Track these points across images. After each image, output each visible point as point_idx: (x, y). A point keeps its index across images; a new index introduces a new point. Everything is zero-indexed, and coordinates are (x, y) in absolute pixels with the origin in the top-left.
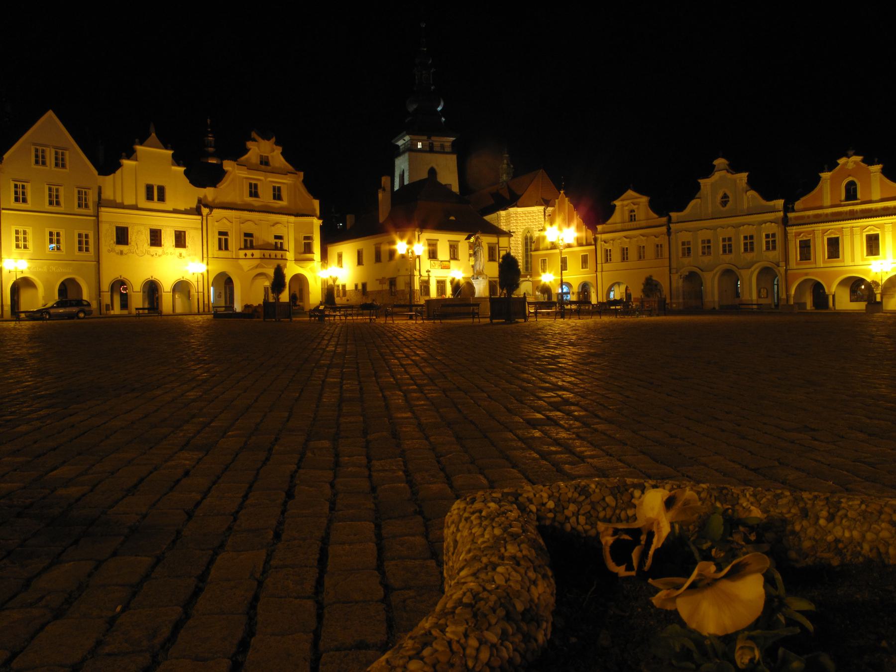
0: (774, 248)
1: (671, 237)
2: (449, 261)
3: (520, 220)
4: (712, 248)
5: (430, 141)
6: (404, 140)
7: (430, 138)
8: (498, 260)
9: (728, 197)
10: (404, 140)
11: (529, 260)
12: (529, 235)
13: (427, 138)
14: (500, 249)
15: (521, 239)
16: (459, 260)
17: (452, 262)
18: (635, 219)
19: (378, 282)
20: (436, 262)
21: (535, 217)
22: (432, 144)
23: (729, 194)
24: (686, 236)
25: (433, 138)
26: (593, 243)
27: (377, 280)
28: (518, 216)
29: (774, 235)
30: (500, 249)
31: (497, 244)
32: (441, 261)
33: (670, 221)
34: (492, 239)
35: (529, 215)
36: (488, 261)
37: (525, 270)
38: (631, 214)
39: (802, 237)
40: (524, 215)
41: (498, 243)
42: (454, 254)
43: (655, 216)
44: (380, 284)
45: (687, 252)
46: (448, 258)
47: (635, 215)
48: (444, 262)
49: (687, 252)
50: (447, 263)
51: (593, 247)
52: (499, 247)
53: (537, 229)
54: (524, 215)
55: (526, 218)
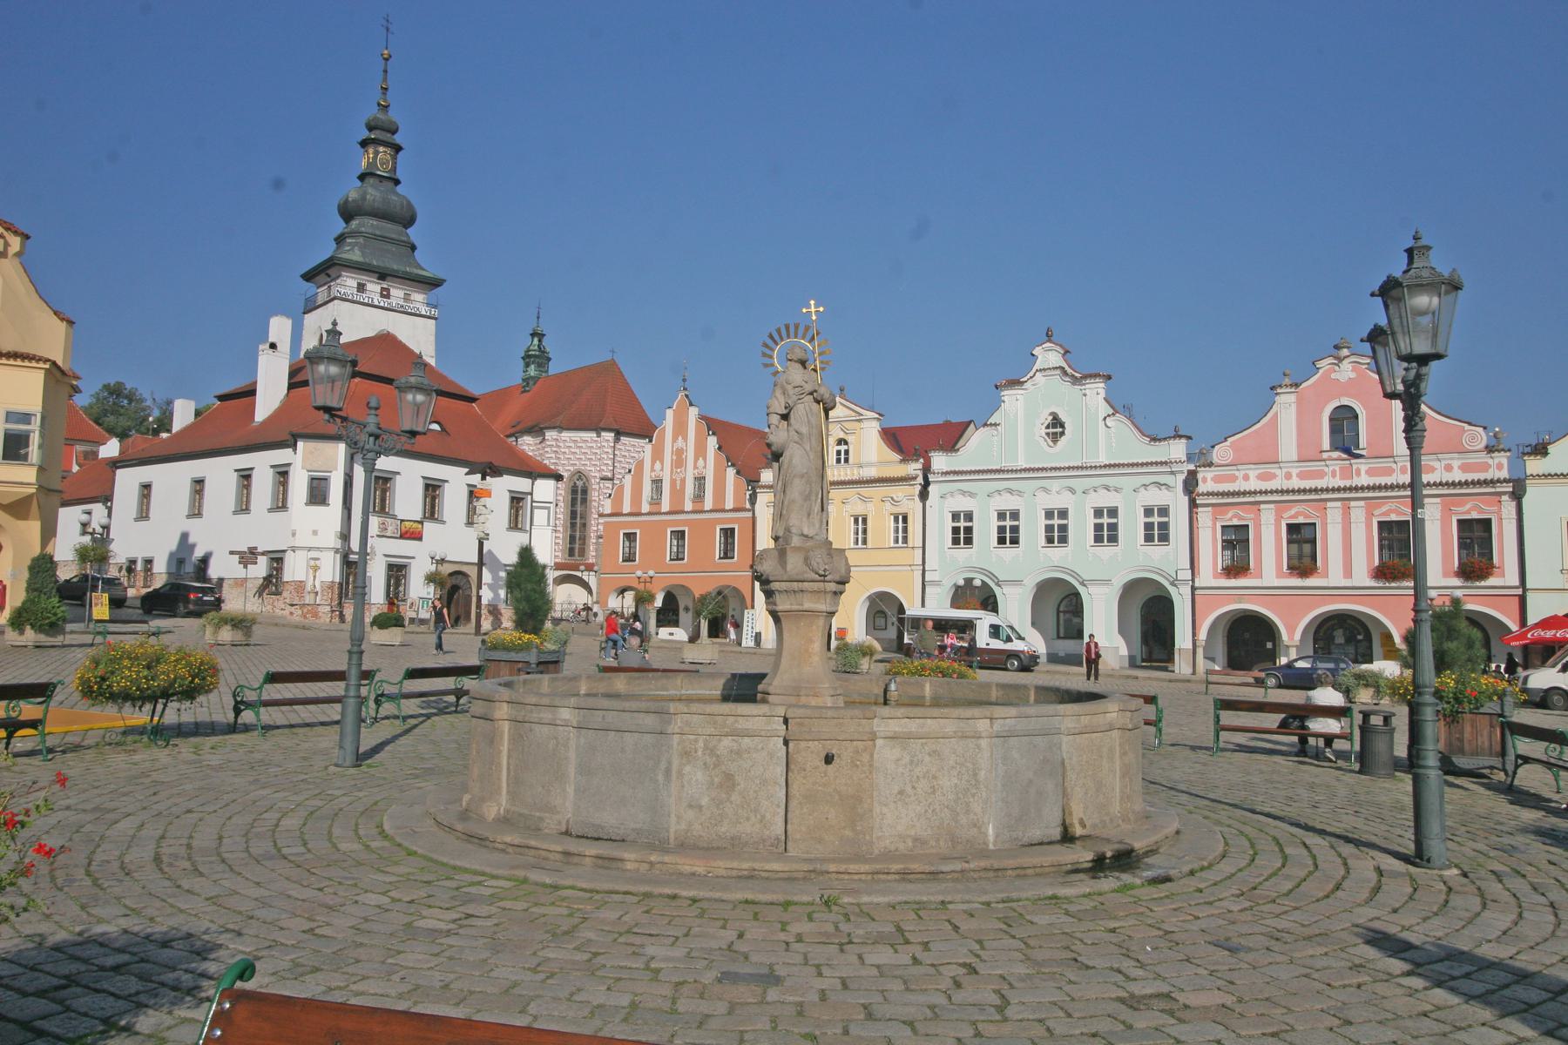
0: (1164, 538)
1: (928, 503)
3: (565, 453)
4: (1070, 528)
5: (385, 286)
6: (329, 276)
8: (528, 529)
9: (1062, 426)
10: (329, 276)
11: (578, 534)
12: (580, 484)
15: (563, 492)
16: (444, 522)
17: (429, 527)
18: (846, 460)
19: (237, 557)
21: (594, 451)
23: (1063, 417)
24: (963, 504)
26: (748, 506)
27: (232, 553)
28: (561, 444)
29: (1164, 511)
31: (527, 494)
32: (402, 521)
33: (927, 469)
34: (521, 484)
35: (583, 445)
37: (567, 556)
38: (839, 448)
39: (1231, 519)
40: (572, 445)
41: (531, 494)
42: (433, 506)
43: (897, 457)
44: (240, 563)
45: (963, 536)
46: (418, 517)
47: (847, 452)
49: (963, 536)
50: (415, 525)
51: (749, 514)
52: (532, 501)
53: (597, 475)
54: (572, 445)
55: (578, 451)
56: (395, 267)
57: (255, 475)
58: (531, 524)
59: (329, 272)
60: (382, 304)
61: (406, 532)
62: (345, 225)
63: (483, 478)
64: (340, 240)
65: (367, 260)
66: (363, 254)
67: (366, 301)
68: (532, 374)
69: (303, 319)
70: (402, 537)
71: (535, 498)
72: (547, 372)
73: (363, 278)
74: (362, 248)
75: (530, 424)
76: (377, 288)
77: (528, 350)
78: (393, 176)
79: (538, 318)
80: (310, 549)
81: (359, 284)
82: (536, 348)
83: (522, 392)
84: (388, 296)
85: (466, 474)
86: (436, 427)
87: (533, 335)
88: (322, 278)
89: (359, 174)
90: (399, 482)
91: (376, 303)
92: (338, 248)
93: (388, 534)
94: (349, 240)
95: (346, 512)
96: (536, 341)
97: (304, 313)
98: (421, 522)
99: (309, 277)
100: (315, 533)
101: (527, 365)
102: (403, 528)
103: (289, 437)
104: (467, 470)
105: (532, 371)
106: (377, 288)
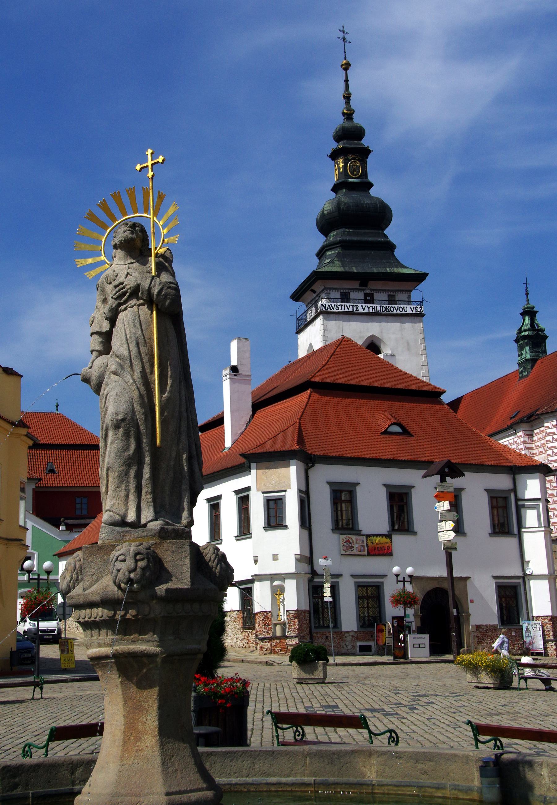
2: (389, 536)
5: (368, 291)
6: (314, 292)
7: (366, 285)
8: (516, 531)
13: (360, 285)
14: (520, 503)
16: (415, 533)
20: (354, 537)
22: (372, 295)
25: (372, 285)
30: (520, 503)
31: (509, 491)
32: (368, 536)
36: (491, 535)
46: (383, 526)
48: (374, 538)
50: (384, 540)
56: (375, 270)
57: (223, 504)
58: (520, 525)
59: (313, 288)
60: (366, 310)
61: (375, 548)
62: (325, 238)
63: (443, 480)
64: (321, 254)
65: (347, 269)
66: (343, 265)
67: (351, 310)
68: (528, 357)
69: (297, 339)
70: (369, 554)
71: (520, 496)
72: (545, 351)
73: (346, 285)
74: (338, 256)
75: (527, 412)
76: (361, 295)
77: (520, 331)
78: (365, 180)
79: (527, 294)
80: (272, 577)
81: (342, 294)
82: (529, 326)
83: (521, 378)
84: (372, 301)
85: (423, 477)
86: (397, 429)
87: (524, 314)
88: (309, 296)
89: (331, 186)
90: (361, 495)
91: (361, 310)
92: (320, 263)
93: (355, 552)
94: (328, 253)
95: (306, 532)
96: (527, 320)
97: (298, 333)
98: (388, 536)
99: (297, 296)
100: (275, 557)
101: (521, 348)
102: (370, 544)
103: (243, 460)
104: (423, 472)
105: (527, 353)
106: (361, 295)
